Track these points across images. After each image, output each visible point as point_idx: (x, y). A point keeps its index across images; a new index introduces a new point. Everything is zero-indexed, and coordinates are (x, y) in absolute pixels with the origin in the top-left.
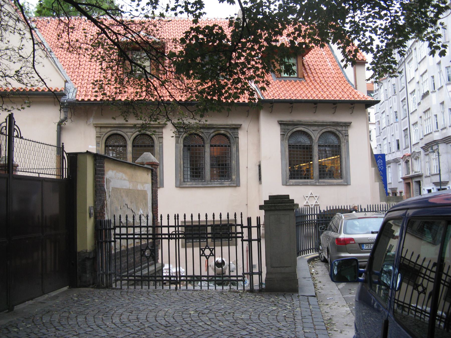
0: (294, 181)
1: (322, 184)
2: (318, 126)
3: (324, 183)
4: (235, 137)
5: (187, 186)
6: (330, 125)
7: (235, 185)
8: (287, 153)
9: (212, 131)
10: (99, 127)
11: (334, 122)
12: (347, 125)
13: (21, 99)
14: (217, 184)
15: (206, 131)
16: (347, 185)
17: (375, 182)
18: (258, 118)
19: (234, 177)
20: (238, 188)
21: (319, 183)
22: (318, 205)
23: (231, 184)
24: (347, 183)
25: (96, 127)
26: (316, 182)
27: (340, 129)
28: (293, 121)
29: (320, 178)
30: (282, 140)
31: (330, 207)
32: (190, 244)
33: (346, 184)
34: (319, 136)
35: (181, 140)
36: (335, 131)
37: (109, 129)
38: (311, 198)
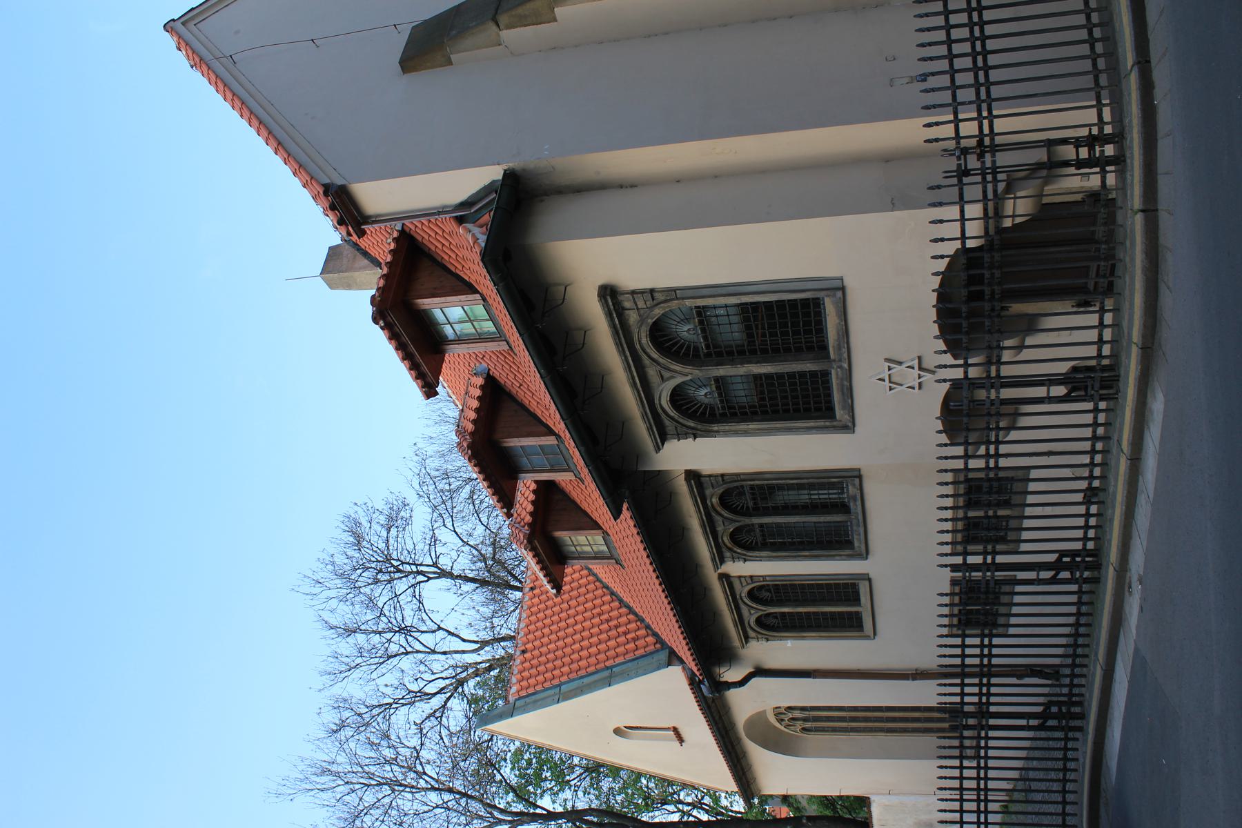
0: (839, 412)
1: (845, 355)
3: (839, 348)
7: (857, 481)
8: (752, 426)
11: (618, 344)
12: (609, 293)
16: (843, 289)
21: (840, 360)
24: (839, 288)
26: (840, 367)
27: (633, 317)
28: (650, 429)
29: (824, 348)
30: (708, 434)
32: (1011, 536)
33: (839, 294)
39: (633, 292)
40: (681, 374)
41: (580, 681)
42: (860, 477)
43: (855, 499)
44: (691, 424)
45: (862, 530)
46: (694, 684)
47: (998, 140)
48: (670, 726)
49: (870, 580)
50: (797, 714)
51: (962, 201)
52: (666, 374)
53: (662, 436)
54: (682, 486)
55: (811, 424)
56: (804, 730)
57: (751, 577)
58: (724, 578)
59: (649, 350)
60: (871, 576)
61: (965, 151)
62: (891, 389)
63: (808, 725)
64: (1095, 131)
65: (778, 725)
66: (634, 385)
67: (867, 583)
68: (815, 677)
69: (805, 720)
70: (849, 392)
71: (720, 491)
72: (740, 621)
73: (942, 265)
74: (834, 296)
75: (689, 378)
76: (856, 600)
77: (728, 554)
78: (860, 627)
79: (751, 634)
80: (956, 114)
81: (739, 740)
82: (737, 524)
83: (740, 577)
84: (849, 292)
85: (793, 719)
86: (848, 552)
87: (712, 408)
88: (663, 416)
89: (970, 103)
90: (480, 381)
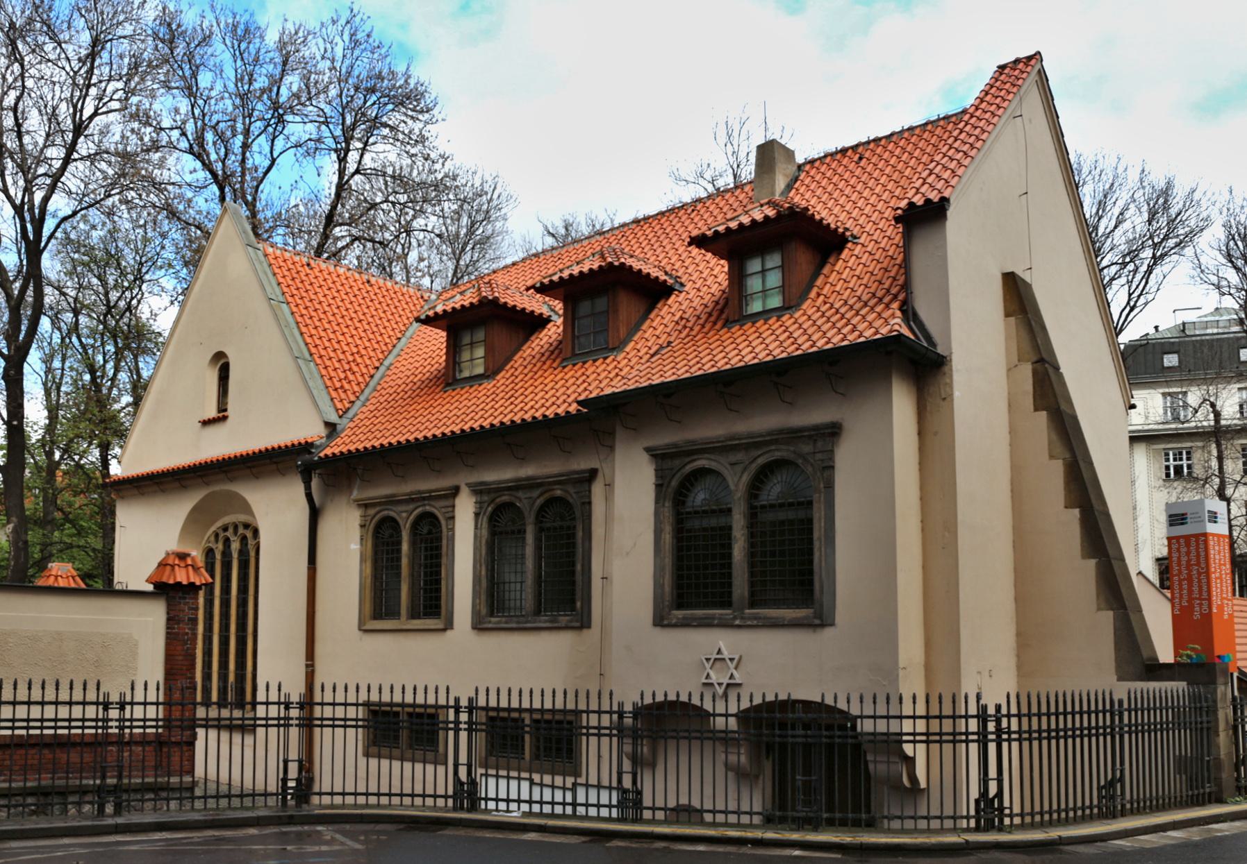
0: (680, 614)
2: (748, 447)
4: (583, 503)
5: (490, 626)
6: (776, 442)
7: (578, 624)
8: (668, 537)
9: (536, 493)
10: (365, 505)
12: (833, 431)
13: (274, 467)
14: (546, 622)
15: (528, 495)
16: (823, 625)
17: (1099, 609)
18: (612, 448)
19: (579, 604)
20: (585, 631)
21: (742, 618)
22: (739, 685)
23: (571, 621)
24: (822, 620)
25: (359, 506)
26: (735, 618)
27: (806, 448)
28: (675, 445)
29: (752, 605)
31: (654, 695)
33: (817, 622)
34: (746, 478)
35: (484, 521)
36: (791, 457)
37: (378, 509)
38: (718, 664)
39: (832, 451)
40: (738, 482)
41: (293, 325)
42: (581, 628)
43: (551, 622)
44: (674, 483)
45: (514, 625)
46: (306, 448)
47: (1005, 745)
48: (230, 412)
49: (444, 630)
50: (235, 546)
51: (927, 717)
52: (739, 468)
53: (659, 456)
54: (582, 464)
55: (667, 589)
56: (209, 553)
57: (453, 518)
58: (456, 491)
59: (766, 456)
60: (449, 633)
61: (998, 722)
62: (708, 660)
63: (218, 556)
64: (1007, 811)
65: (219, 524)
66: (732, 438)
67: (441, 626)
68: (309, 569)
69: (226, 554)
70: (685, 624)
71: (573, 498)
72: (391, 501)
73: (842, 705)
74: (815, 617)
75: (732, 487)
76: (414, 615)
77: (485, 498)
78: (377, 616)
79: (372, 512)
80: (961, 717)
81: (207, 484)
82: (526, 514)
83: (454, 506)
84: (819, 630)
85: (227, 541)
86: (484, 611)
87: (684, 503)
88: (687, 460)
89: (1030, 726)
90: (670, 281)
